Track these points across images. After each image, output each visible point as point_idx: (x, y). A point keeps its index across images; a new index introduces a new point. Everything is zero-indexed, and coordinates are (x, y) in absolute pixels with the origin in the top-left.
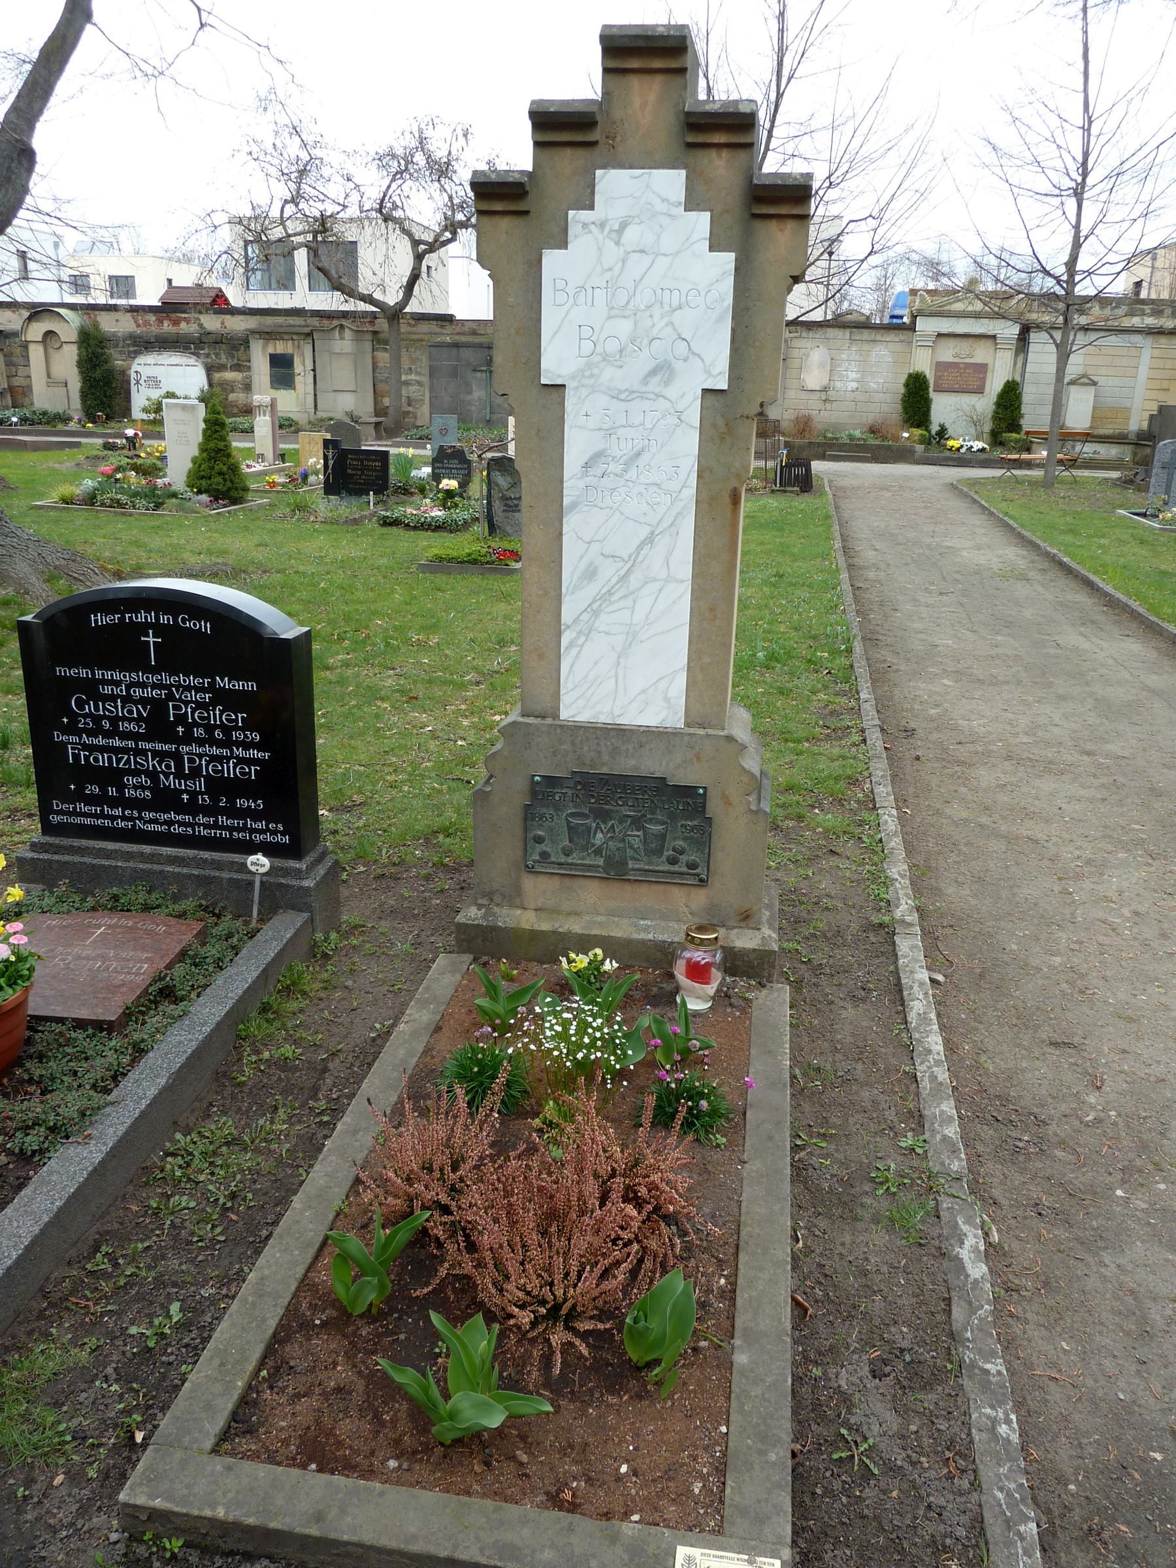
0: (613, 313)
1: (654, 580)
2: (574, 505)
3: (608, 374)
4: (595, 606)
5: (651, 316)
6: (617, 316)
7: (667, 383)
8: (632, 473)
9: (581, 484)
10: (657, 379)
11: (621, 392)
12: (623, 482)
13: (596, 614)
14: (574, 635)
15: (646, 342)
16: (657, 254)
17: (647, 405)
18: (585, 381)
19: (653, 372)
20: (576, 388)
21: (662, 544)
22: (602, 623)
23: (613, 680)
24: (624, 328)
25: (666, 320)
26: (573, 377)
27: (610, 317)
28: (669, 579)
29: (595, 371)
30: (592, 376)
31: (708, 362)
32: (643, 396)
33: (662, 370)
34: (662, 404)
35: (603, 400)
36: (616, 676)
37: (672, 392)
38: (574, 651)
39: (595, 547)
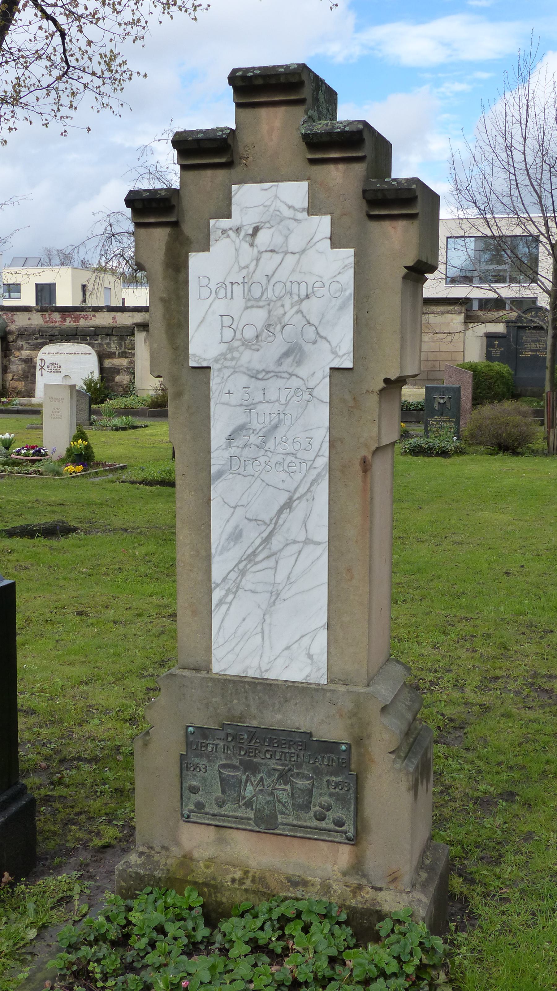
0: (249, 304)
1: (295, 542)
2: (220, 474)
3: (247, 357)
4: (241, 566)
5: (283, 306)
6: (253, 307)
7: (299, 363)
8: (271, 444)
9: (226, 454)
10: (290, 359)
11: (258, 372)
12: (262, 452)
13: (243, 573)
14: (223, 592)
15: (278, 328)
16: (286, 253)
17: (281, 383)
18: (228, 363)
19: (286, 354)
20: (219, 370)
21: (300, 508)
22: (248, 582)
23: (259, 637)
24: (259, 316)
25: (295, 309)
26: (216, 360)
27: (247, 308)
28: (307, 541)
29: (236, 354)
30: (233, 359)
31: (334, 344)
32: (277, 375)
33: (294, 353)
34: (295, 382)
35: (243, 380)
36: (263, 632)
37: (303, 371)
38: (224, 607)
39: (240, 511)
